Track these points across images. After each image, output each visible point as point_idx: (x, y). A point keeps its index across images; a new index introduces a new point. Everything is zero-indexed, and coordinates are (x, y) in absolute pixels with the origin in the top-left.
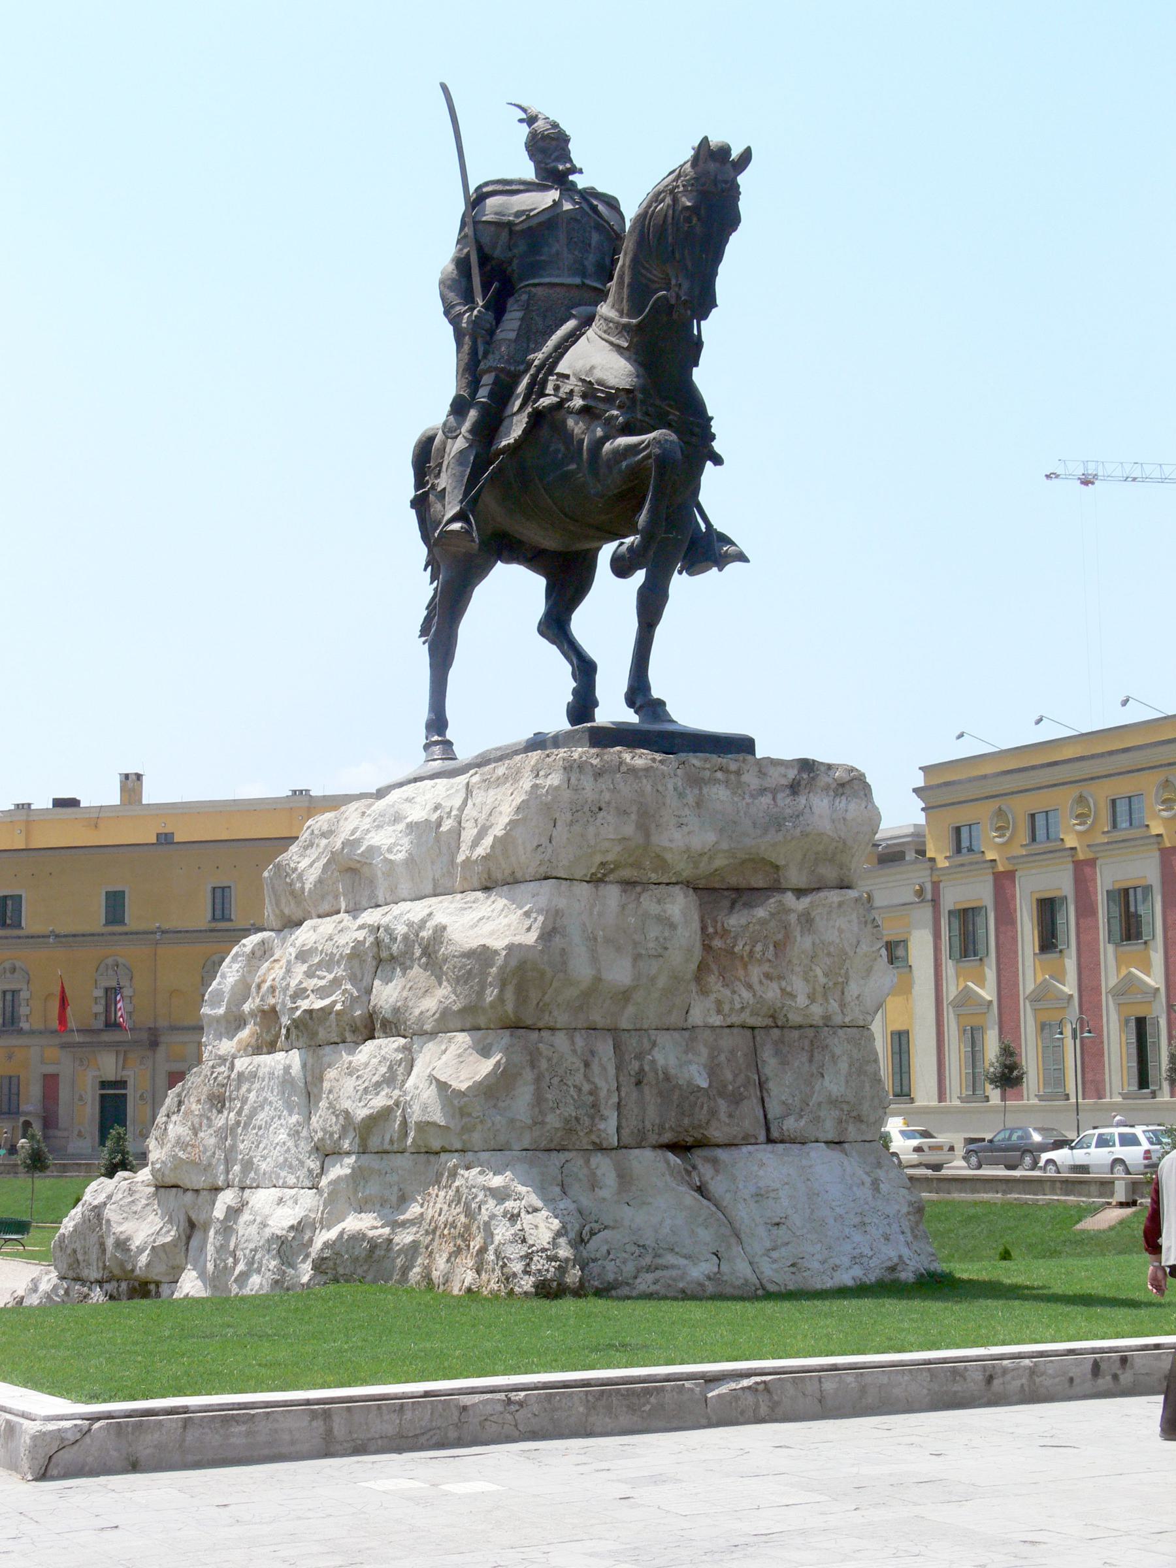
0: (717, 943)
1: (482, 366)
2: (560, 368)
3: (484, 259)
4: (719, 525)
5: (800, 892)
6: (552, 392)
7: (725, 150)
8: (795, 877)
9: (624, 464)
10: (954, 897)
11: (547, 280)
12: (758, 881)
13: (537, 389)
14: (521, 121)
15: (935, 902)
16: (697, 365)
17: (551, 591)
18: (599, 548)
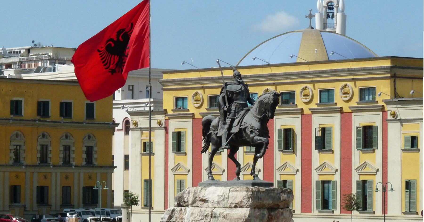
0: (270, 217)
1: (228, 117)
3: (228, 98)
5: (282, 209)
8: (281, 206)
10: (174, 126)
12: (276, 207)
15: (166, 129)
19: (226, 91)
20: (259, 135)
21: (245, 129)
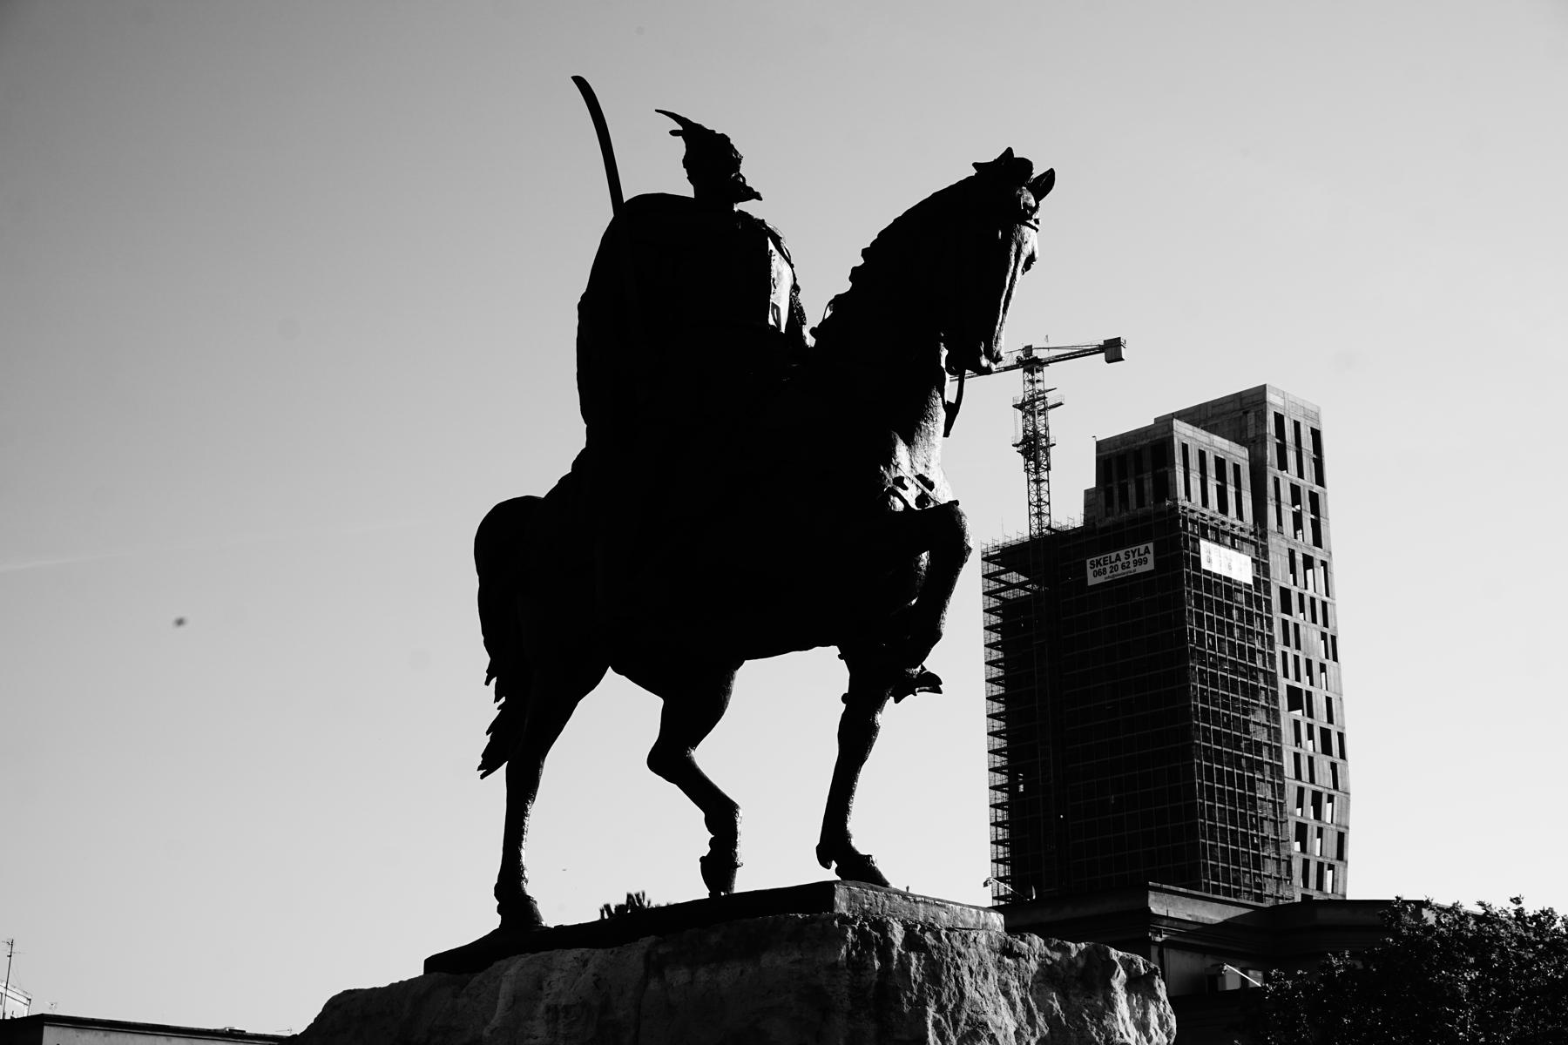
7: (1026, 165)
14: (674, 133)
17: (669, 719)
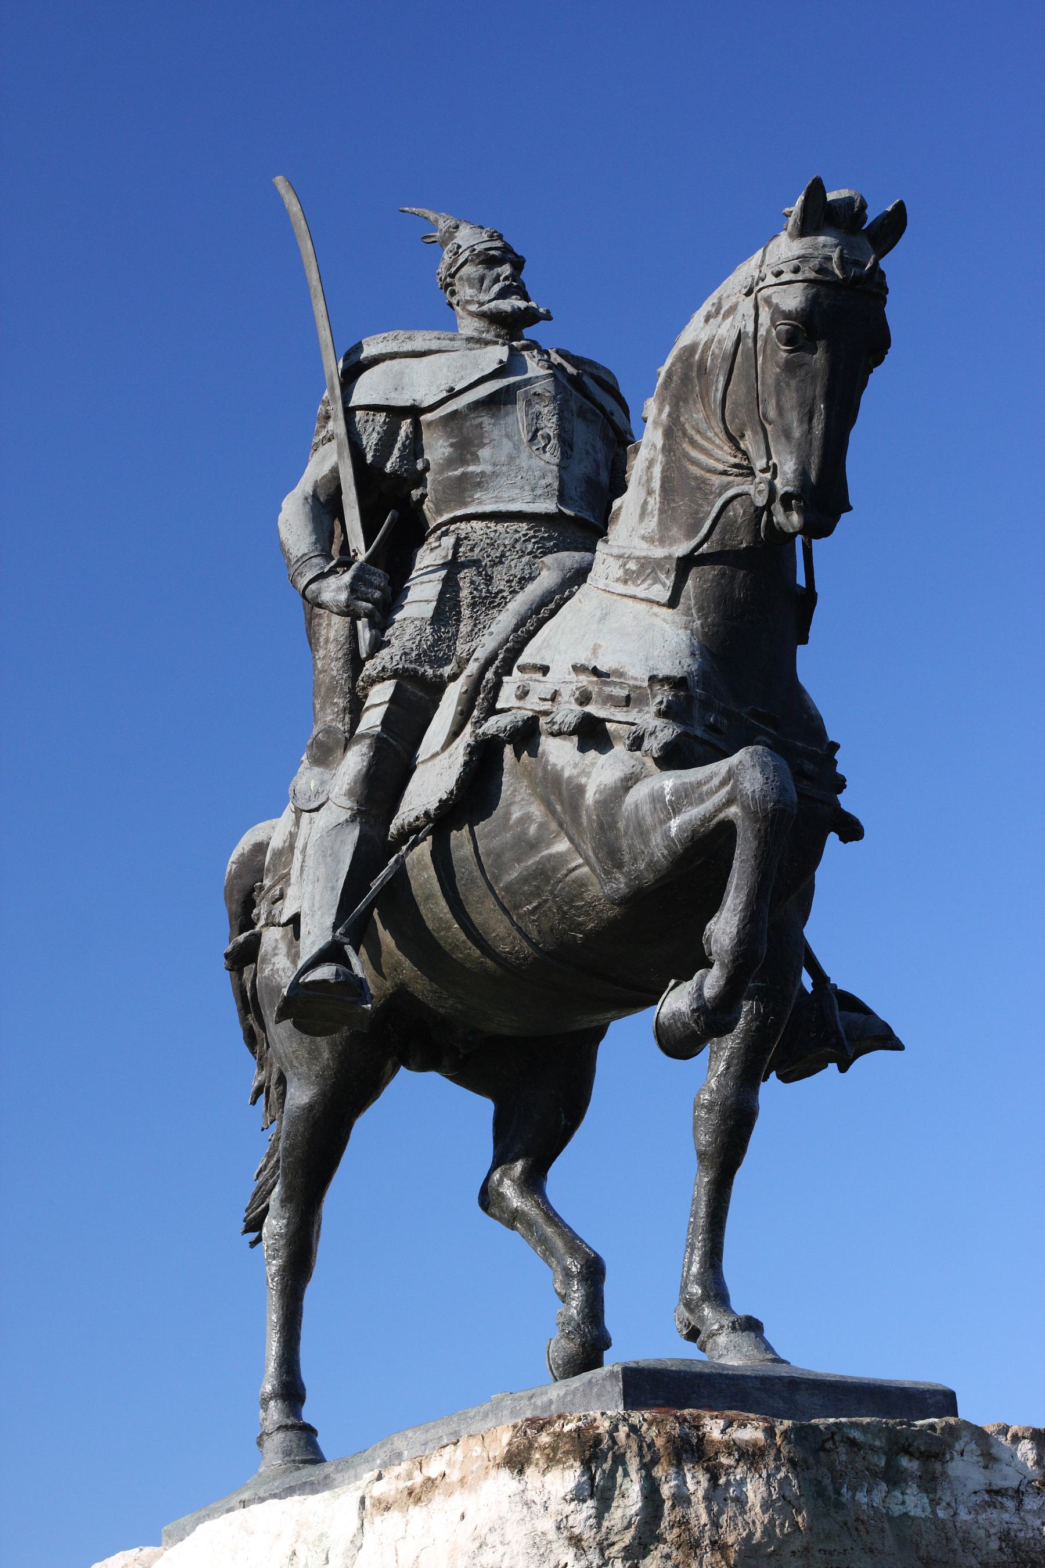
2: (529, 655)
3: (367, 475)
4: (841, 979)
6: (514, 703)
9: (674, 824)
11: (488, 508)
13: (481, 698)
16: (804, 640)
18: (599, 1033)
19: (349, 413)
20: (671, 758)
21: (527, 735)
